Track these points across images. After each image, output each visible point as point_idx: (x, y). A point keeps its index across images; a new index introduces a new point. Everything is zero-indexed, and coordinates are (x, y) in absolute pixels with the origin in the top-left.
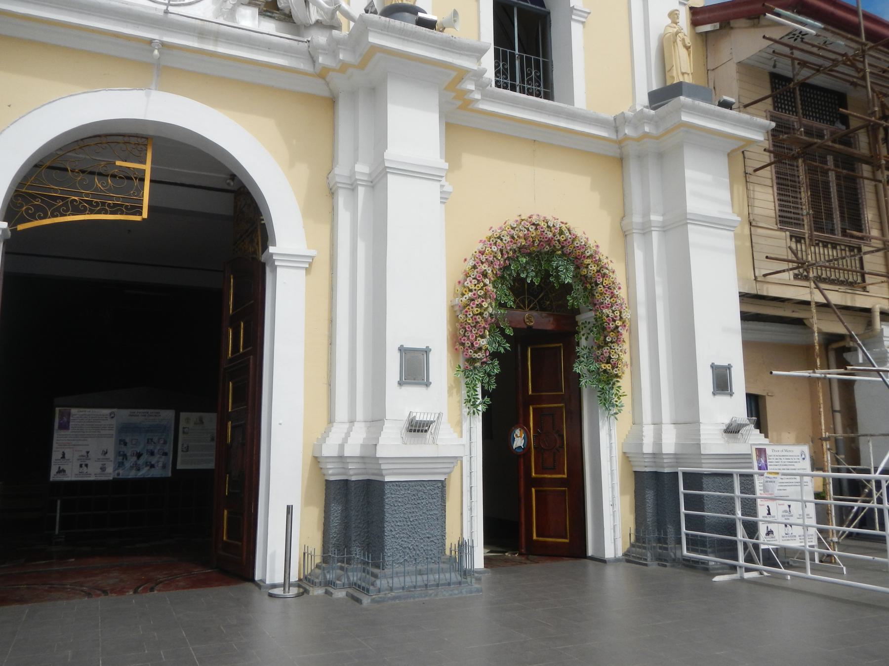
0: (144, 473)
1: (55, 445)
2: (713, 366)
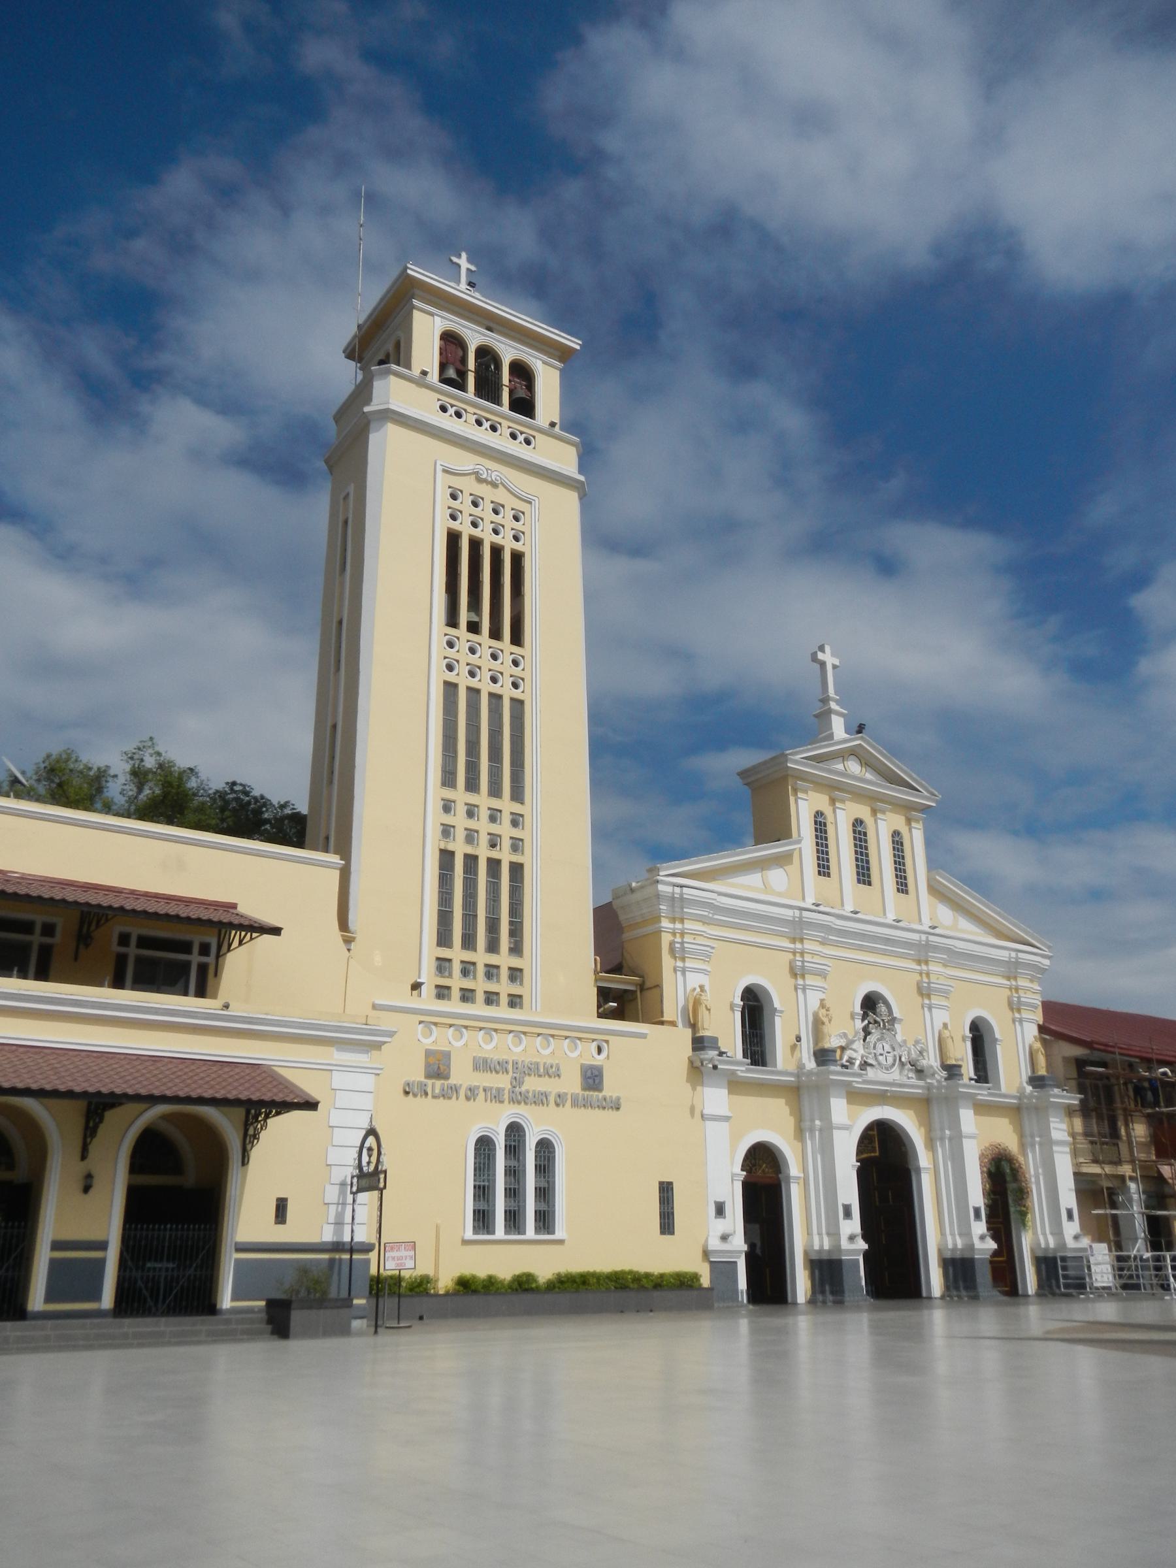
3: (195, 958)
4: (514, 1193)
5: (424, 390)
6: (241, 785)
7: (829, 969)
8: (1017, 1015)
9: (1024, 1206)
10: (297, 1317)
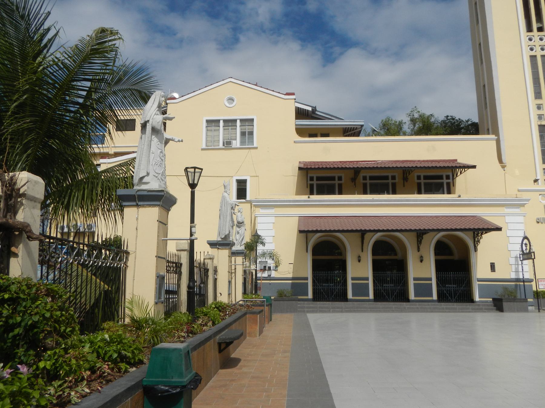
3: (445, 181)
6: (451, 116)
10: (505, 305)
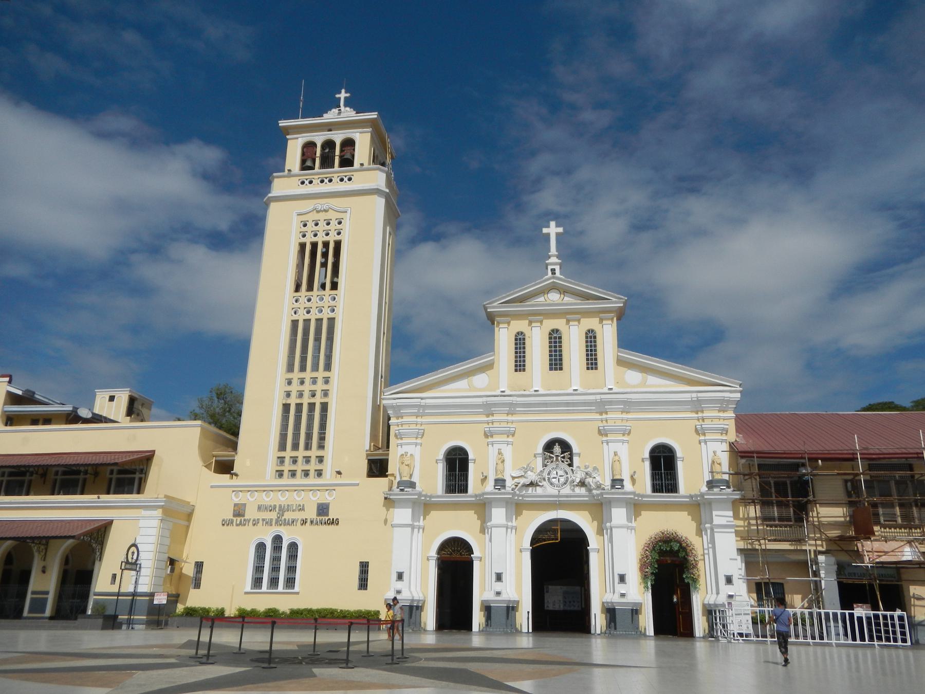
0: (572, 608)
1: (545, 598)
2: (725, 576)
3: (137, 476)
4: (275, 569)
5: (292, 178)
7: (511, 429)
8: (702, 438)
9: (693, 574)
